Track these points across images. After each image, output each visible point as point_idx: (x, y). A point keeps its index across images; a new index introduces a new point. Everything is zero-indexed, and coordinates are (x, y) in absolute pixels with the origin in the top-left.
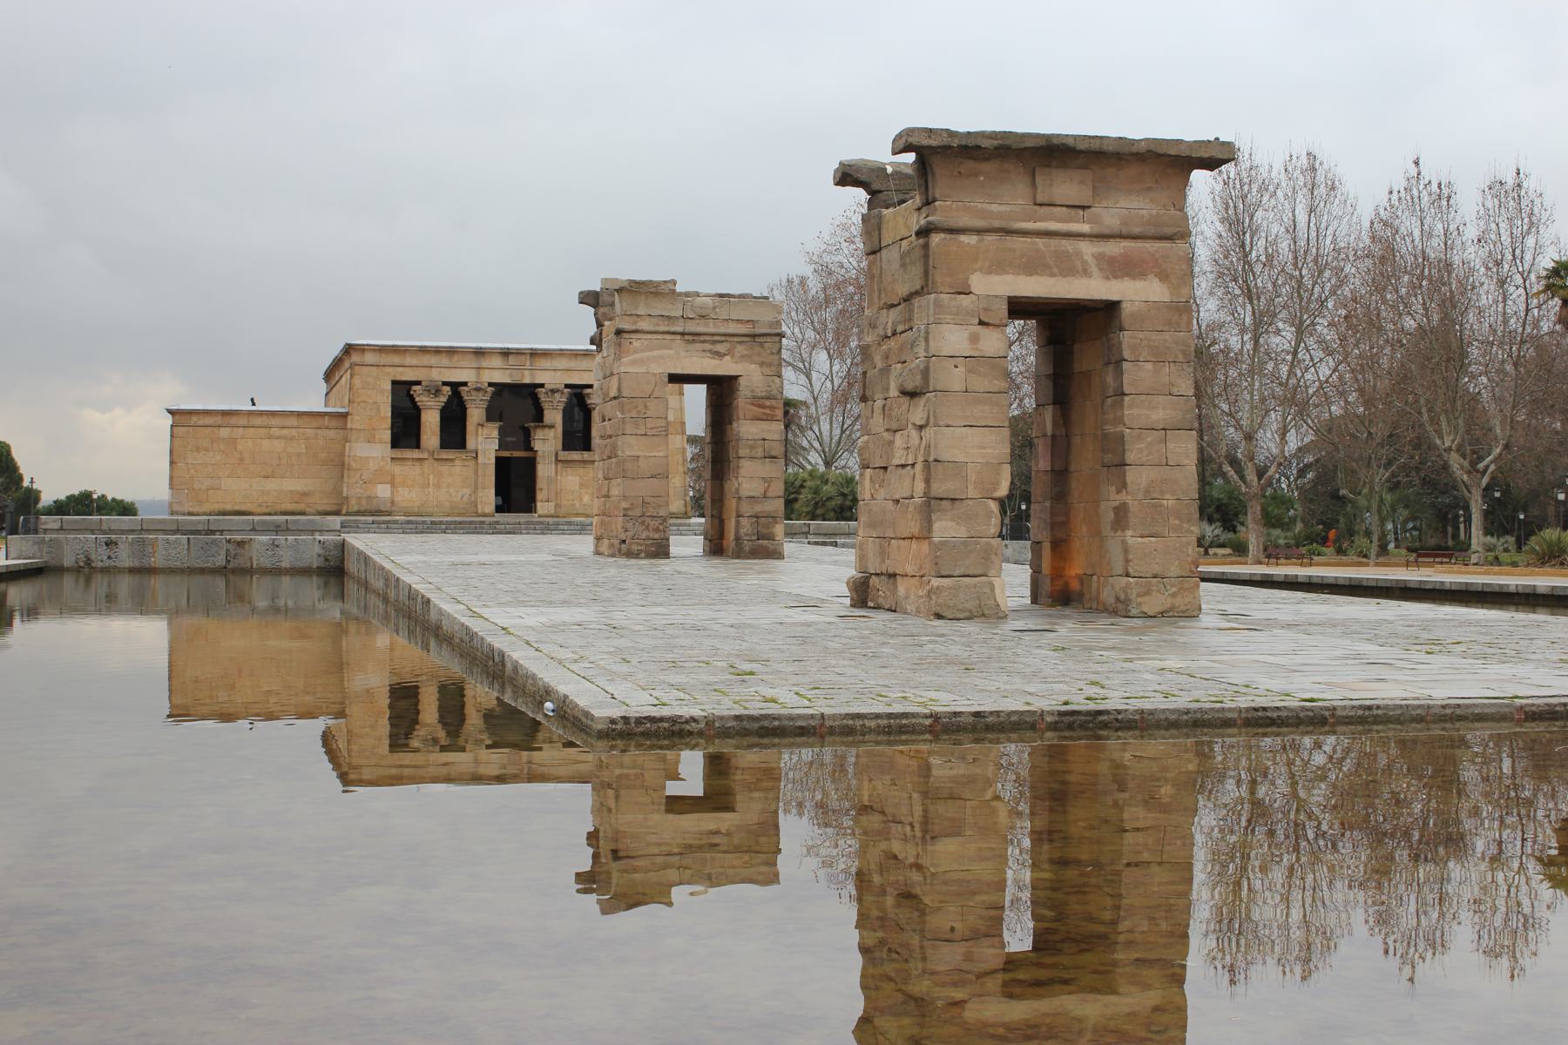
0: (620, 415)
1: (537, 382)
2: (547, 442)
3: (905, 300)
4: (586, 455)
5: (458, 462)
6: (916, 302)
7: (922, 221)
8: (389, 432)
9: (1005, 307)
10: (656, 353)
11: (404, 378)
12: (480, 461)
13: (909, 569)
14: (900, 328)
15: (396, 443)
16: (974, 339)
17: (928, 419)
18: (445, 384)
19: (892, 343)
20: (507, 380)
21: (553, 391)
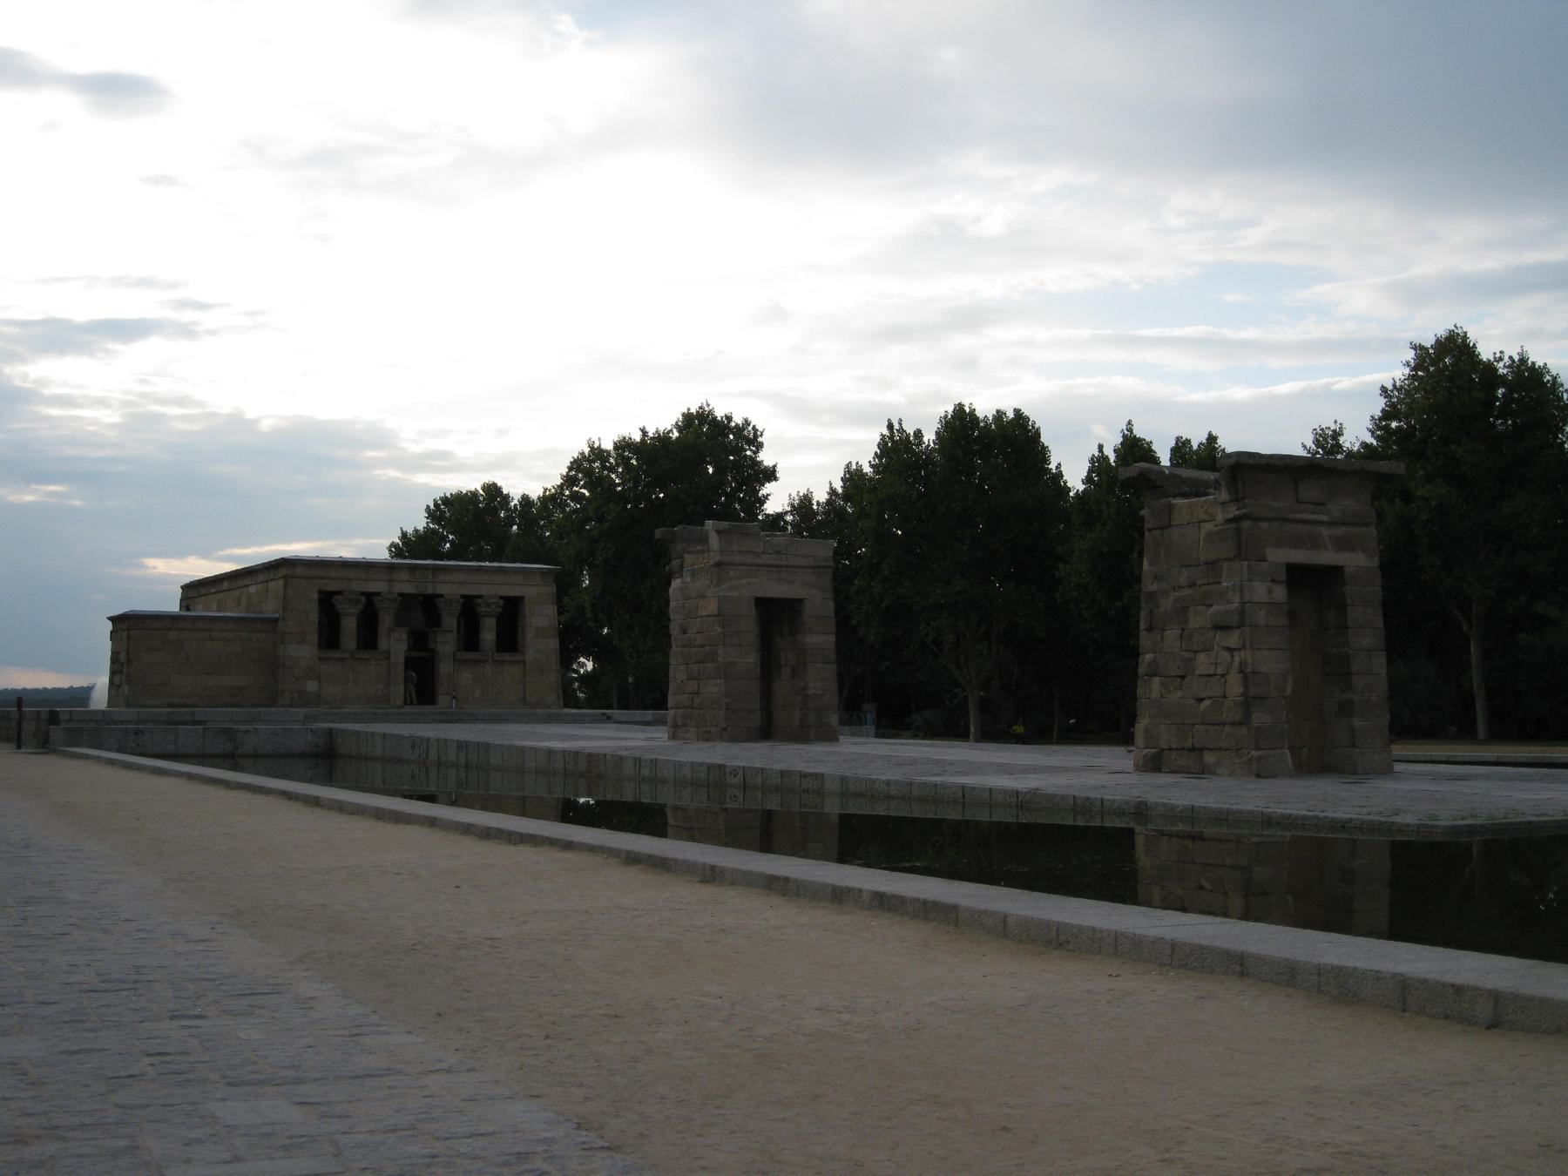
0: (719, 629)
1: (438, 592)
2: (446, 643)
3: (1205, 564)
4: (478, 656)
5: (373, 662)
6: (1225, 566)
7: (1233, 511)
8: (316, 635)
9: (1284, 570)
10: (744, 581)
11: (329, 589)
12: (392, 660)
13: (1223, 745)
14: (1199, 583)
15: (320, 645)
16: (1270, 591)
17: (1244, 644)
18: (363, 594)
19: (1186, 592)
20: (414, 591)
21: (451, 601)
